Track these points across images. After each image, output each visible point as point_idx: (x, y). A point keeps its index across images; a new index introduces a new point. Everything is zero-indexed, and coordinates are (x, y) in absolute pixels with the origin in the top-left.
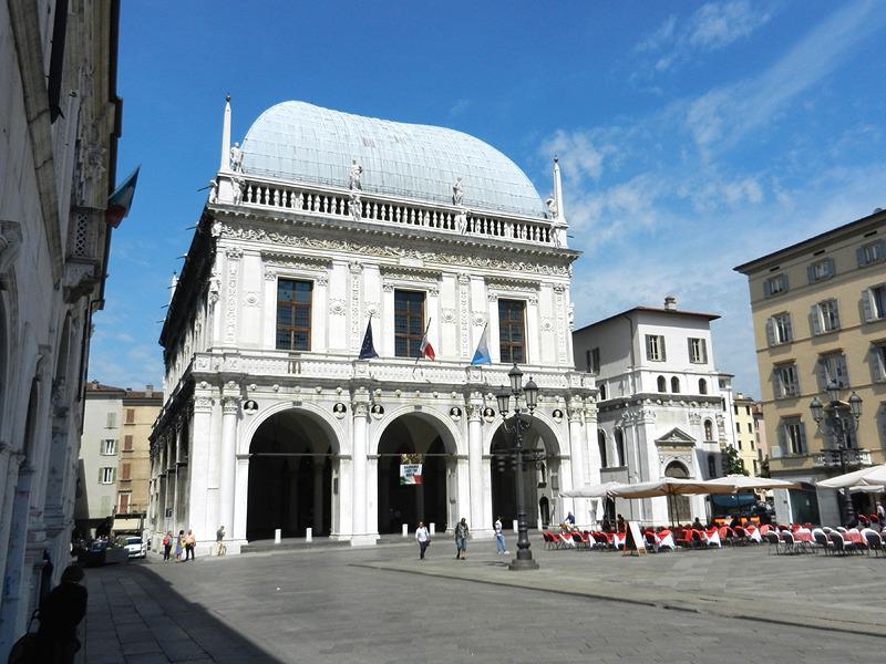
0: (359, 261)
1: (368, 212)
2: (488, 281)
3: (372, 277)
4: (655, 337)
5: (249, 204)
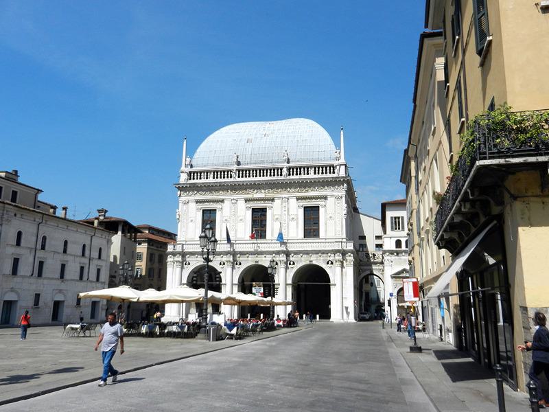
0: (235, 198)
1: (241, 175)
2: (298, 199)
3: (241, 204)
4: (399, 218)
5: (192, 181)
